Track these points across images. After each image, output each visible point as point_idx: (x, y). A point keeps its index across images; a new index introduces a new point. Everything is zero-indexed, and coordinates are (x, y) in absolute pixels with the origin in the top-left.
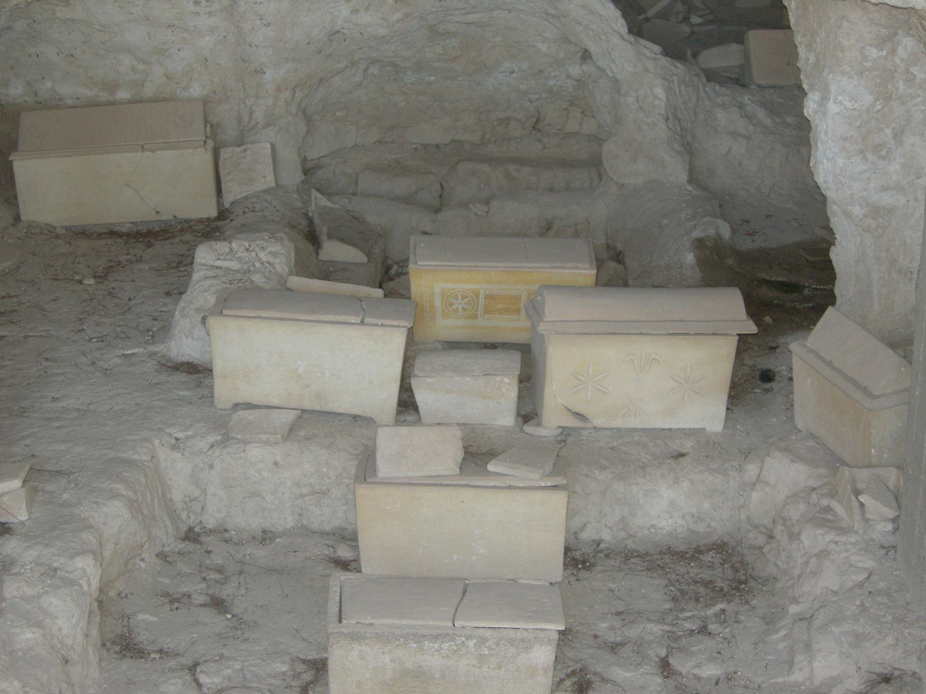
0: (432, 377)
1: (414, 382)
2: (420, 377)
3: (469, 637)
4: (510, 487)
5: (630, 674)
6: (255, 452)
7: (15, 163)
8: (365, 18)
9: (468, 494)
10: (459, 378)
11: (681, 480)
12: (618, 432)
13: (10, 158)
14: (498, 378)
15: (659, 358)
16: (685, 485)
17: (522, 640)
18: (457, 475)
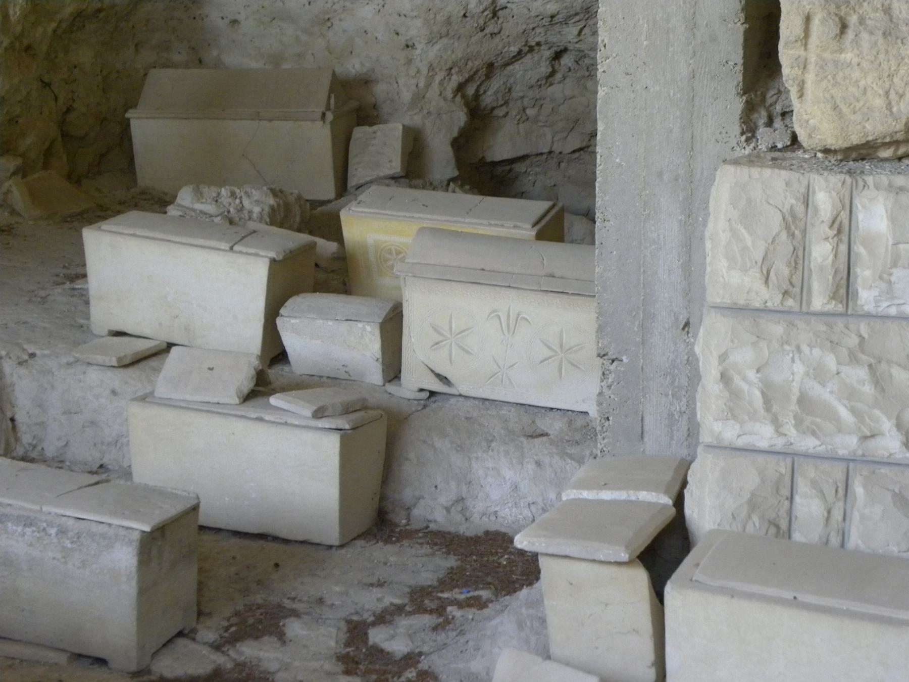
0: (296, 317)
1: (279, 321)
2: (286, 317)
3: (50, 524)
5: (304, 632)
6: (94, 375)
7: (133, 123)
9: (239, 426)
10: (321, 321)
11: (527, 460)
13: (127, 115)
14: (360, 325)
15: (528, 318)
16: (530, 467)
17: (103, 536)
18: (237, 404)
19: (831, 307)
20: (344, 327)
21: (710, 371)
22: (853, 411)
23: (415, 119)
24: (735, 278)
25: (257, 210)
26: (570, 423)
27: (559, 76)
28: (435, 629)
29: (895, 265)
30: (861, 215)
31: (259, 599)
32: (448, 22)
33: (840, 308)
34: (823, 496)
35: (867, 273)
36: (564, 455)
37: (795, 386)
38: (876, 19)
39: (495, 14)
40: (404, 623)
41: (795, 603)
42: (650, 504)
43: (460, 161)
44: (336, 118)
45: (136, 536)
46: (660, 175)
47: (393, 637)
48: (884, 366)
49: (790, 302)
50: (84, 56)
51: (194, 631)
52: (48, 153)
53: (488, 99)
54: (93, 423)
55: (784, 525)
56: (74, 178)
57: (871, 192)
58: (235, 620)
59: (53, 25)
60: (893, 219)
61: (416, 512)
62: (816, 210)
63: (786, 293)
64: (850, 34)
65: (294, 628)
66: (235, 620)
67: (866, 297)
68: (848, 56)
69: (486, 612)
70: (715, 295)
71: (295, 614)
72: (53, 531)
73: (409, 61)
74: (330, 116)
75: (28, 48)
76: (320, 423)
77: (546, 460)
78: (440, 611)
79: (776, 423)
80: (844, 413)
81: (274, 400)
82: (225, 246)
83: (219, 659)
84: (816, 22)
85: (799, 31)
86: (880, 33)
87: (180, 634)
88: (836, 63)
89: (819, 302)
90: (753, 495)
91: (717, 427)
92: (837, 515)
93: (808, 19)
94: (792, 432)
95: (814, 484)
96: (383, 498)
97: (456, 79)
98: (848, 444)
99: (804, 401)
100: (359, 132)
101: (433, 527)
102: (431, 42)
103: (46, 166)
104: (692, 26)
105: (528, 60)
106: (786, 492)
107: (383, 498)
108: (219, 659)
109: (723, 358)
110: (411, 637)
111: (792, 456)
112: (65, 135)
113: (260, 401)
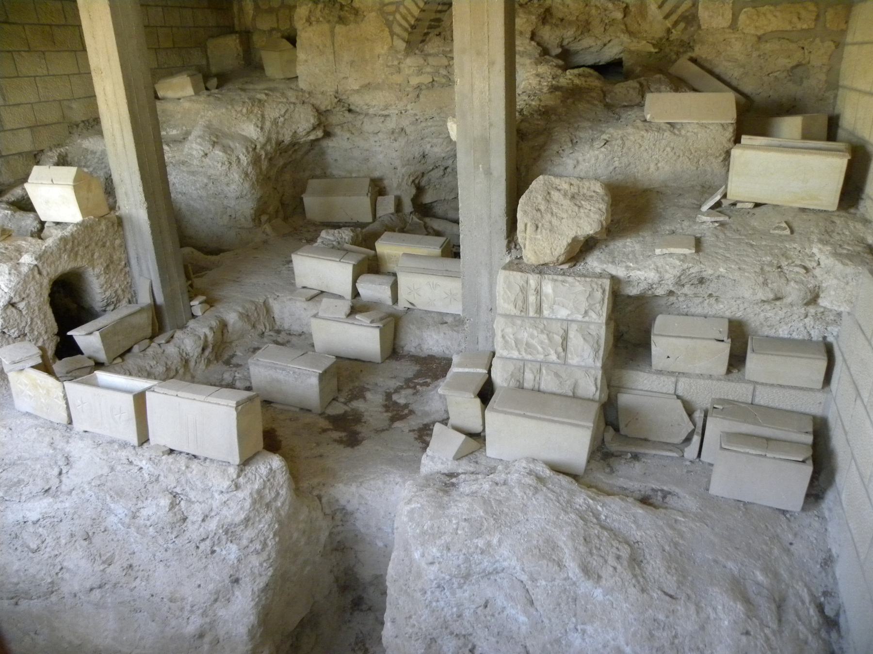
1: (357, 284)
4: (361, 325)
6: (298, 304)
8: (436, 150)
9: (347, 326)
12: (427, 312)
16: (442, 335)
19: (535, 315)
20: (378, 287)
21: (499, 334)
22: (542, 347)
23: (398, 193)
24: (506, 306)
25: (347, 238)
26: (455, 318)
27: (446, 175)
28: (414, 394)
29: (554, 304)
30: (544, 288)
31: (356, 384)
32: (408, 160)
33: (538, 316)
34: (533, 373)
35: (546, 306)
36: (453, 330)
37: (525, 340)
38: (547, 225)
39: (424, 157)
40: (403, 392)
41: (524, 416)
42: (481, 373)
43: (414, 207)
44: (372, 194)
45: (318, 374)
46: (481, 263)
47: (400, 398)
48: (551, 334)
49: (523, 314)
50: (287, 176)
51: (337, 397)
52: (277, 212)
53: (423, 183)
54: (299, 319)
55: (521, 381)
56: (285, 219)
57: (547, 281)
58: (350, 393)
59: (276, 170)
60: (554, 291)
61: (406, 348)
62: (530, 285)
63: (521, 311)
64: (539, 230)
65: (369, 395)
66: (350, 393)
67: (546, 313)
68: (539, 237)
69: (430, 388)
70: (500, 311)
71: (368, 390)
72: (291, 372)
73: (395, 174)
74: (369, 194)
75: (269, 178)
76: (373, 325)
77: (447, 332)
78: (414, 388)
79: (519, 351)
80: (539, 348)
81: (358, 317)
82: (338, 260)
83: (346, 408)
84: (529, 225)
85: (523, 228)
86: (548, 230)
87: (334, 399)
88: (535, 239)
89: (532, 314)
90: (512, 372)
91: (501, 351)
92: (537, 378)
93: (526, 225)
94: (524, 354)
95: (531, 369)
96: (394, 344)
97: (412, 179)
98: (540, 357)
99: (527, 344)
100: (380, 198)
101: (411, 353)
102: (403, 166)
103: (277, 217)
104: (490, 217)
105: (436, 171)
106: (522, 371)
107: (394, 344)
108: (346, 408)
109: (502, 331)
110: (406, 398)
111: (524, 360)
112: (282, 204)
113: (353, 316)
